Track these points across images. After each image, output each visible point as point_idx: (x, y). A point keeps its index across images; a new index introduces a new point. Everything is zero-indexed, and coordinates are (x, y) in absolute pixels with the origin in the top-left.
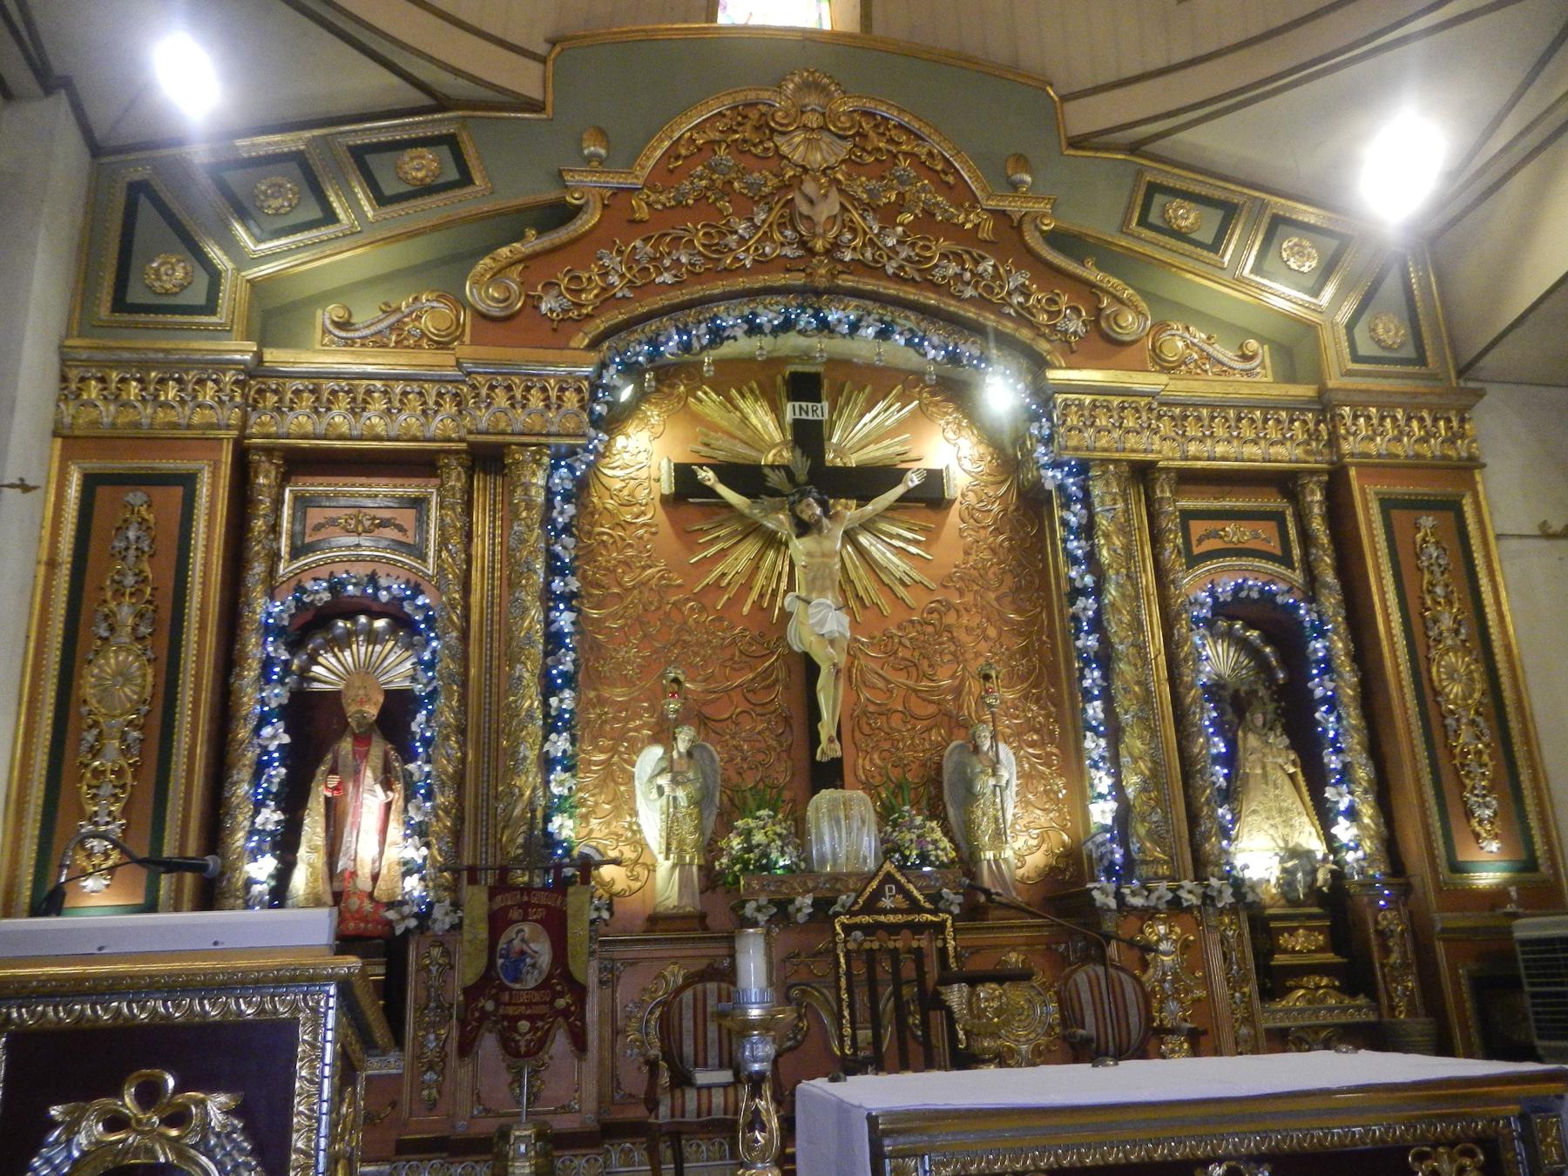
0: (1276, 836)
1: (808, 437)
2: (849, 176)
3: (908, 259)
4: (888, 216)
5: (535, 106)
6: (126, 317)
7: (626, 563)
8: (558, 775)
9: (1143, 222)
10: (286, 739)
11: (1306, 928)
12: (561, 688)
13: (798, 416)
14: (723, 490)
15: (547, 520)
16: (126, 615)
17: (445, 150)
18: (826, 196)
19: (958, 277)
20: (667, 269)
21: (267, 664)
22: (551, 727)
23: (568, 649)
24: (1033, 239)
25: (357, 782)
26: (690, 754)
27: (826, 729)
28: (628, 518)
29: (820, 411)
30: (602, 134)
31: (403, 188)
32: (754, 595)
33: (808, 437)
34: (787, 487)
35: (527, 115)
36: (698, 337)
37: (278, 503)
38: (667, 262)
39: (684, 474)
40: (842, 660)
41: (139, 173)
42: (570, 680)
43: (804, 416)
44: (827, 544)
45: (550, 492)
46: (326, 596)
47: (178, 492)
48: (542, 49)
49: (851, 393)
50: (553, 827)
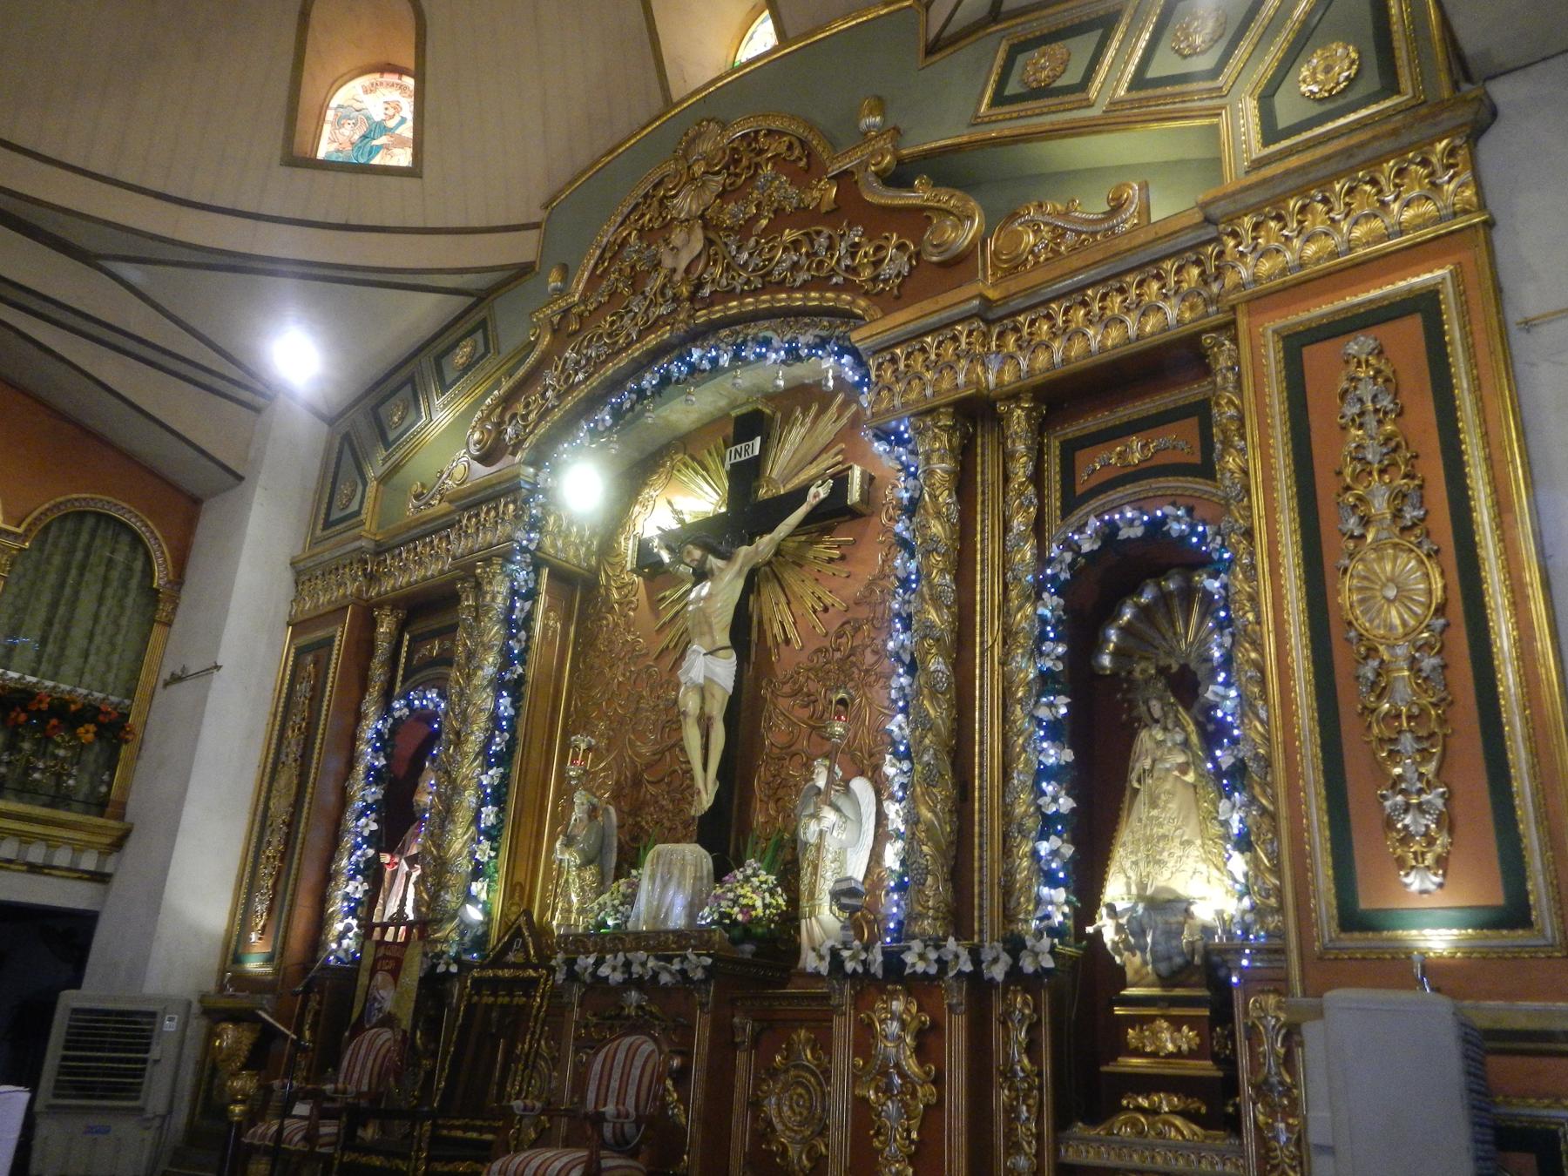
0: (1134, 878)
8: (486, 845)
10: (374, 827)
11: (1167, 1018)
33: (744, 477)
40: (717, 709)
43: (738, 459)
45: (514, 592)
48: (539, 216)
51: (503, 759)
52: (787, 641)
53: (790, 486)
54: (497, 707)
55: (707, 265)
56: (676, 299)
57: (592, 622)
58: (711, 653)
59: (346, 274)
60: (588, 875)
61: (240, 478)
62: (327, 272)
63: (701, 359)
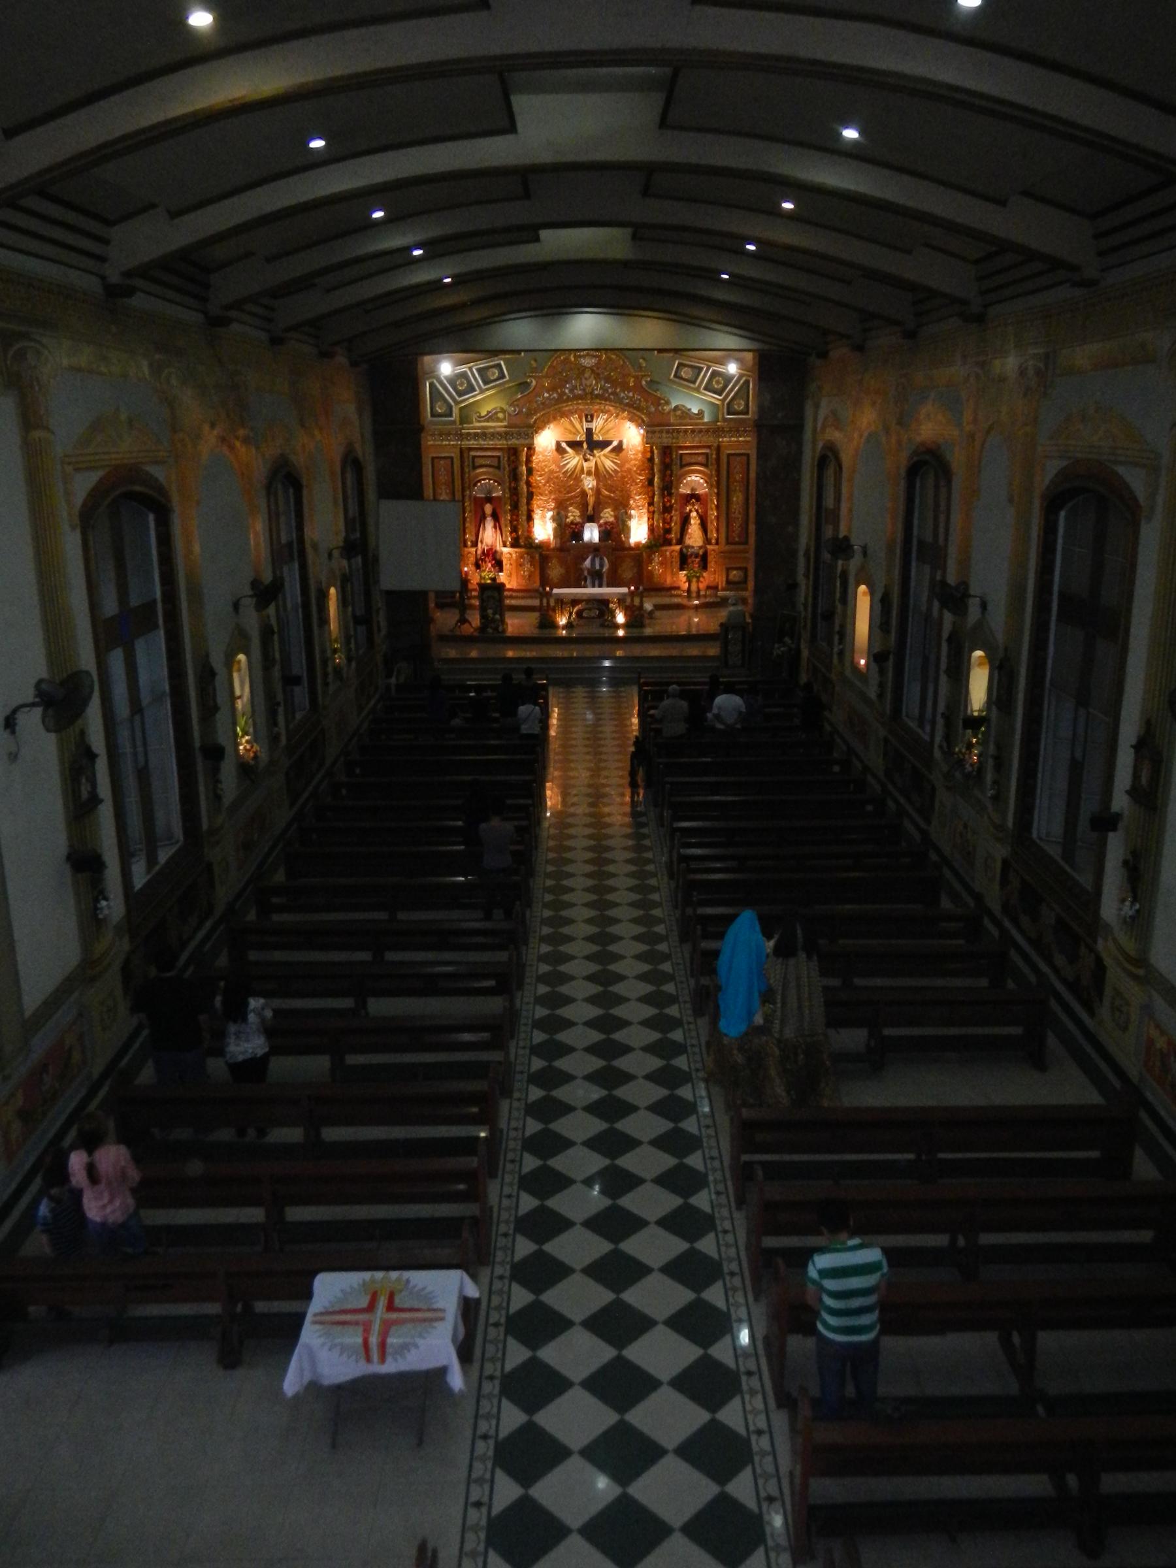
1: (589, 432)
2: (598, 368)
3: (612, 394)
4: (608, 379)
7: (546, 466)
9: (675, 376)
14: (568, 449)
18: (590, 377)
19: (623, 397)
24: (644, 383)
27: (590, 508)
28: (546, 454)
29: (590, 425)
30: (536, 361)
32: (575, 474)
33: (589, 432)
37: (468, 457)
39: (558, 444)
41: (431, 380)
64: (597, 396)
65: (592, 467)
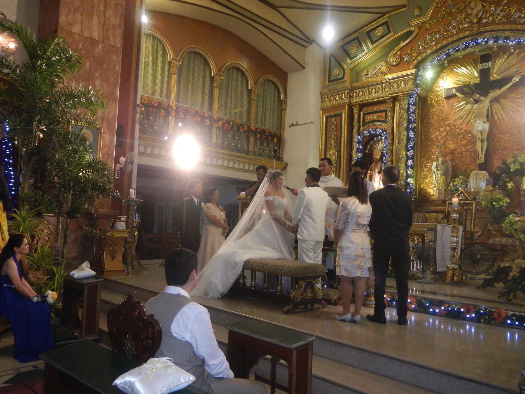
3: (504, 16)
5: (404, 6)
6: (330, 83)
12: (410, 150)
13: (481, 68)
15: (408, 111)
16: (332, 142)
17: (385, 26)
19: (520, 17)
20: (434, 41)
21: (358, 149)
22: (408, 158)
23: (412, 141)
25: (375, 172)
26: (443, 163)
30: (420, 8)
31: (378, 38)
33: (484, 74)
34: (470, 92)
35: (401, 10)
36: (443, 57)
38: (434, 39)
40: (485, 136)
42: (412, 148)
43: (483, 68)
44: (481, 105)
45: (409, 104)
46: (368, 134)
47: (340, 117)
49: (501, 56)
50: (409, 180)
51: (412, 148)
52: (503, 119)
53: (503, 75)
54: (408, 135)
55: (483, 12)
56: (471, 22)
57: (427, 111)
58: (484, 123)
59: (348, 9)
60: (443, 177)
61: (304, 68)
62: (344, 9)
63: (482, 41)
64: (486, 25)
65: (483, 108)
